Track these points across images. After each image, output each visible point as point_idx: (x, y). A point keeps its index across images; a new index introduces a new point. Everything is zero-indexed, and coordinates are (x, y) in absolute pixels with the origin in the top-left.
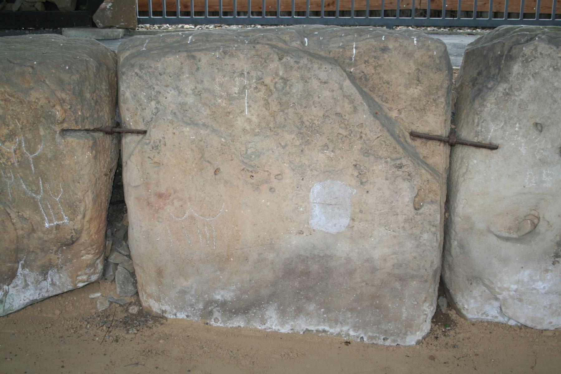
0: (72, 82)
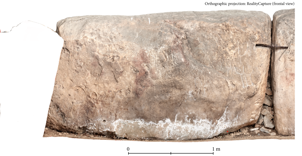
0: (262, 26)
